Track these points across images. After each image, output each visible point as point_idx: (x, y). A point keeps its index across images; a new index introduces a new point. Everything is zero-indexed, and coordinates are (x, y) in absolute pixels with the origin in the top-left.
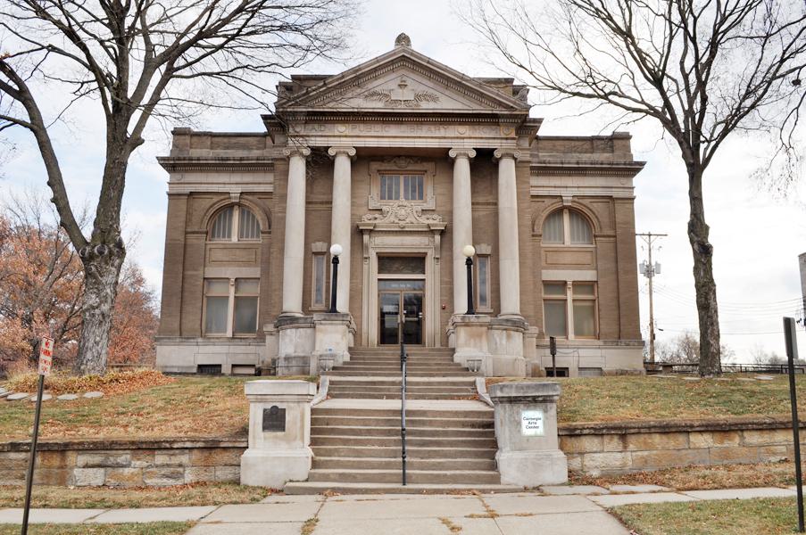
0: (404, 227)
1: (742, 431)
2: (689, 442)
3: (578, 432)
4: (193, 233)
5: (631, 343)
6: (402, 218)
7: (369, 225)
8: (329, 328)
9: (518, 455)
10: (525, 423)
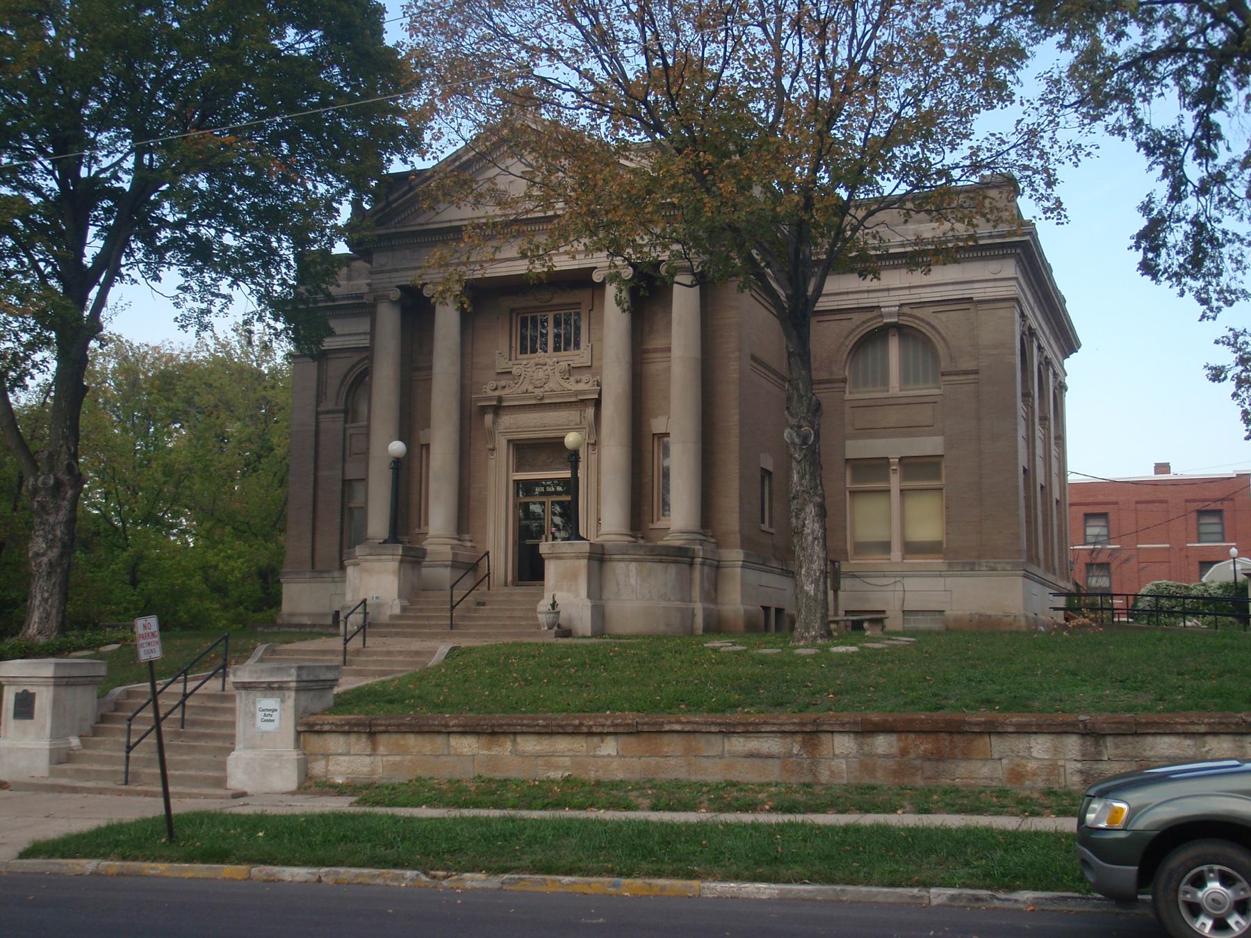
0: (542, 398)
1: (515, 734)
2: (449, 746)
3: (317, 728)
4: (328, 412)
5: (999, 567)
6: (538, 383)
7: (490, 399)
8: (377, 565)
9: (249, 754)
10: (260, 715)
